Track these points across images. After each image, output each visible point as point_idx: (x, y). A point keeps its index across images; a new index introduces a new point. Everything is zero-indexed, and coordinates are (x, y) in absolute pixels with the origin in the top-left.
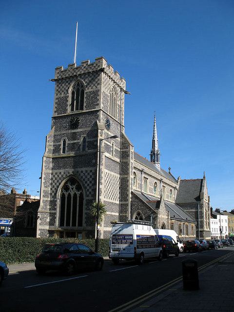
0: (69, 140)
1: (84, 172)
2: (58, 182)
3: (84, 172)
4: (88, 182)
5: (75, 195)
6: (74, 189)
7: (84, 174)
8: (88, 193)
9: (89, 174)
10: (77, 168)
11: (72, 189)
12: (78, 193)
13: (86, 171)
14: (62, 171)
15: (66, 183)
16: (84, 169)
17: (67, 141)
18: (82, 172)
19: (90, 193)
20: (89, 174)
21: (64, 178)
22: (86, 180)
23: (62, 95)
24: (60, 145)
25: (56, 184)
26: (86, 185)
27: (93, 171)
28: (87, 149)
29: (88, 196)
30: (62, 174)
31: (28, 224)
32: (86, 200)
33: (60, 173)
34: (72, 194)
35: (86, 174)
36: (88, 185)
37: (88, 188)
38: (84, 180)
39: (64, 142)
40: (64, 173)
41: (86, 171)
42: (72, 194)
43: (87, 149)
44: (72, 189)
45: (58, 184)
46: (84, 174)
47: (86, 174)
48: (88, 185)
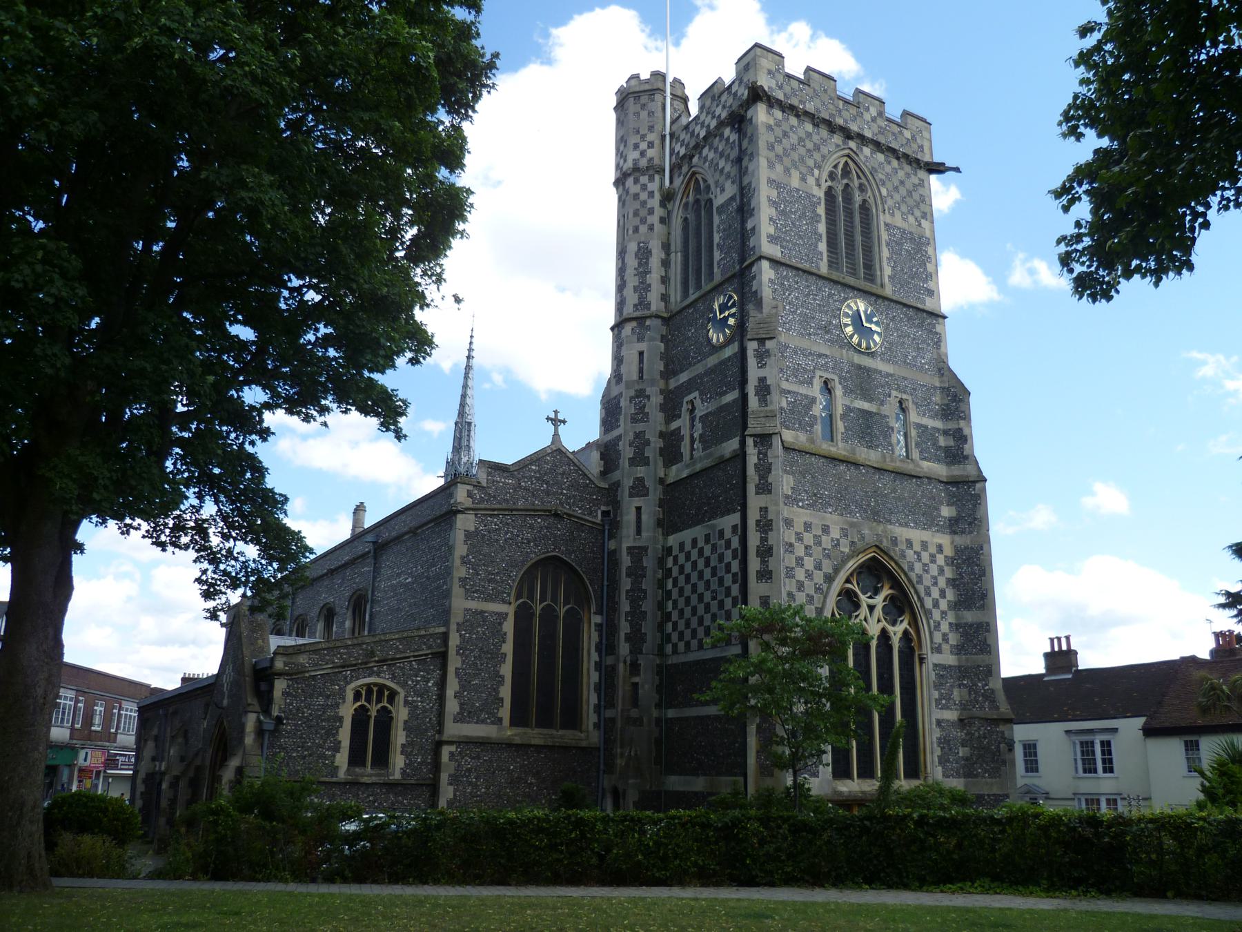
0: (847, 391)
1: (917, 547)
2: (818, 567)
3: (917, 547)
4: (935, 593)
5: (884, 635)
6: (878, 611)
7: (918, 554)
8: (938, 638)
9: (933, 559)
10: (889, 521)
11: (871, 608)
12: (896, 632)
13: (924, 545)
14: (835, 521)
15: (848, 581)
16: (917, 535)
17: (839, 392)
18: (910, 544)
19: (945, 638)
20: (933, 559)
21: (855, 553)
22: (927, 581)
23: (795, 182)
24: (813, 401)
25: (809, 575)
26: (928, 603)
27: (948, 551)
28: (916, 454)
29: (938, 650)
30: (835, 533)
31: (356, 758)
32: (935, 665)
33: (826, 530)
34: (874, 629)
35: (925, 557)
36: (936, 605)
37: (936, 615)
38: (920, 577)
39: (827, 387)
40: (844, 532)
41: (924, 545)
42: (874, 629)
43: (916, 454)
44: (871, 608)
45: (819, 577)
46: (918, 554)
47: (925, 557)
48: (936, 605)
